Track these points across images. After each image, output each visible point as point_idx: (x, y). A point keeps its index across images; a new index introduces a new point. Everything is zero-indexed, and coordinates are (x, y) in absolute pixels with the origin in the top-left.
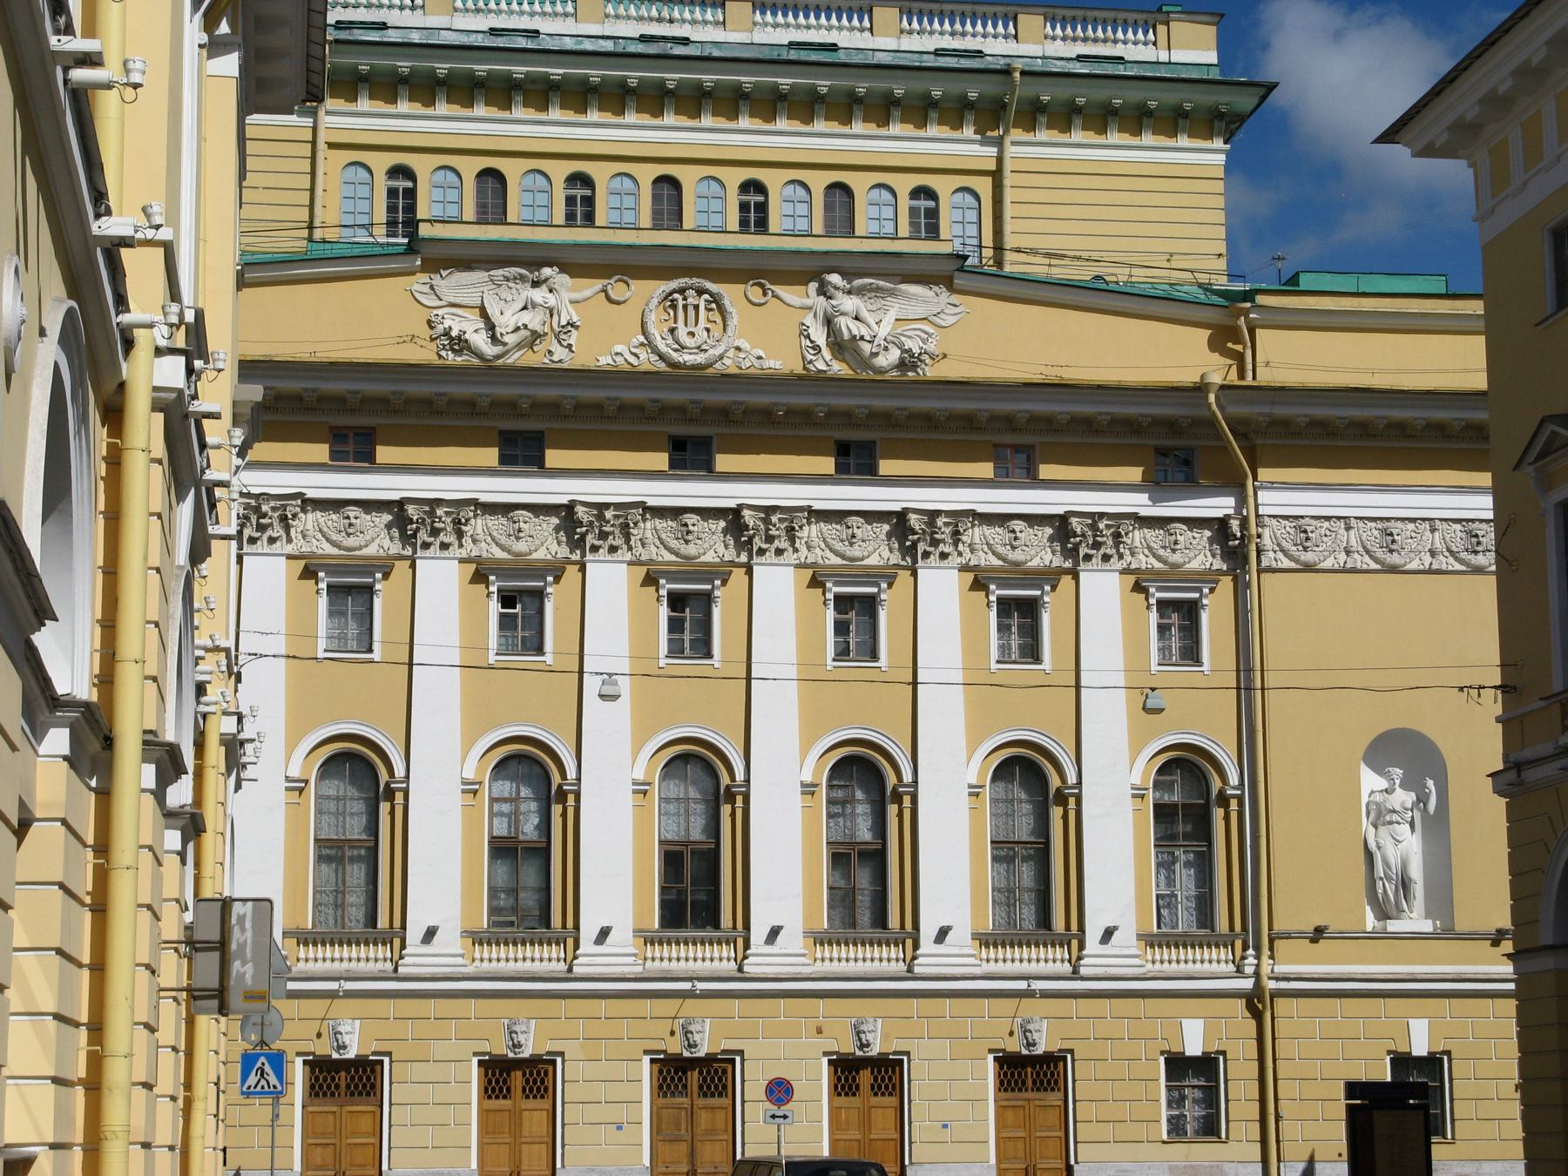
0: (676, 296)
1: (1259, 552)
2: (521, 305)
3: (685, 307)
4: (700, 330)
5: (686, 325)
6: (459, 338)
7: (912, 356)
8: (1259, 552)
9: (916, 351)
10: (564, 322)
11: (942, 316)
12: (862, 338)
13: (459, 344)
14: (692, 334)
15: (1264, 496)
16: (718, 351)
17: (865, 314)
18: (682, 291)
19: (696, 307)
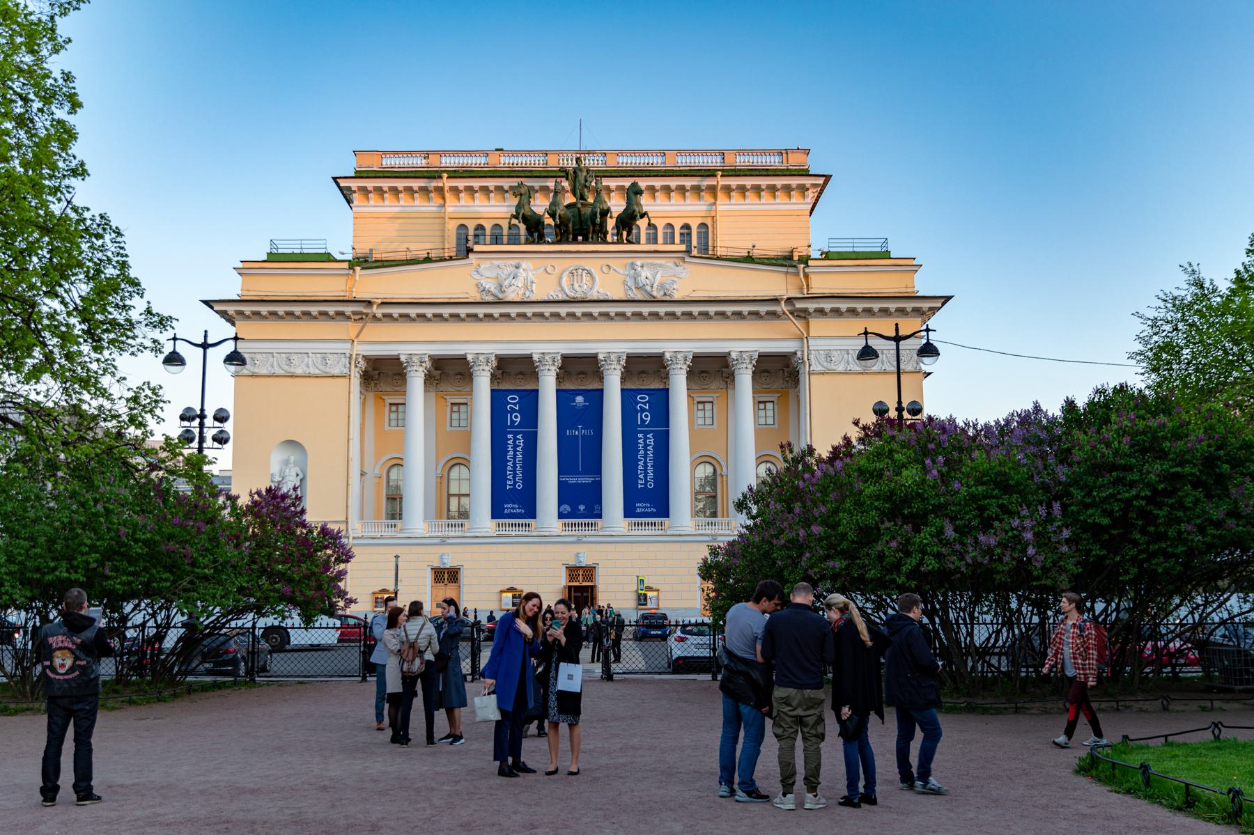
8: (810, 365)
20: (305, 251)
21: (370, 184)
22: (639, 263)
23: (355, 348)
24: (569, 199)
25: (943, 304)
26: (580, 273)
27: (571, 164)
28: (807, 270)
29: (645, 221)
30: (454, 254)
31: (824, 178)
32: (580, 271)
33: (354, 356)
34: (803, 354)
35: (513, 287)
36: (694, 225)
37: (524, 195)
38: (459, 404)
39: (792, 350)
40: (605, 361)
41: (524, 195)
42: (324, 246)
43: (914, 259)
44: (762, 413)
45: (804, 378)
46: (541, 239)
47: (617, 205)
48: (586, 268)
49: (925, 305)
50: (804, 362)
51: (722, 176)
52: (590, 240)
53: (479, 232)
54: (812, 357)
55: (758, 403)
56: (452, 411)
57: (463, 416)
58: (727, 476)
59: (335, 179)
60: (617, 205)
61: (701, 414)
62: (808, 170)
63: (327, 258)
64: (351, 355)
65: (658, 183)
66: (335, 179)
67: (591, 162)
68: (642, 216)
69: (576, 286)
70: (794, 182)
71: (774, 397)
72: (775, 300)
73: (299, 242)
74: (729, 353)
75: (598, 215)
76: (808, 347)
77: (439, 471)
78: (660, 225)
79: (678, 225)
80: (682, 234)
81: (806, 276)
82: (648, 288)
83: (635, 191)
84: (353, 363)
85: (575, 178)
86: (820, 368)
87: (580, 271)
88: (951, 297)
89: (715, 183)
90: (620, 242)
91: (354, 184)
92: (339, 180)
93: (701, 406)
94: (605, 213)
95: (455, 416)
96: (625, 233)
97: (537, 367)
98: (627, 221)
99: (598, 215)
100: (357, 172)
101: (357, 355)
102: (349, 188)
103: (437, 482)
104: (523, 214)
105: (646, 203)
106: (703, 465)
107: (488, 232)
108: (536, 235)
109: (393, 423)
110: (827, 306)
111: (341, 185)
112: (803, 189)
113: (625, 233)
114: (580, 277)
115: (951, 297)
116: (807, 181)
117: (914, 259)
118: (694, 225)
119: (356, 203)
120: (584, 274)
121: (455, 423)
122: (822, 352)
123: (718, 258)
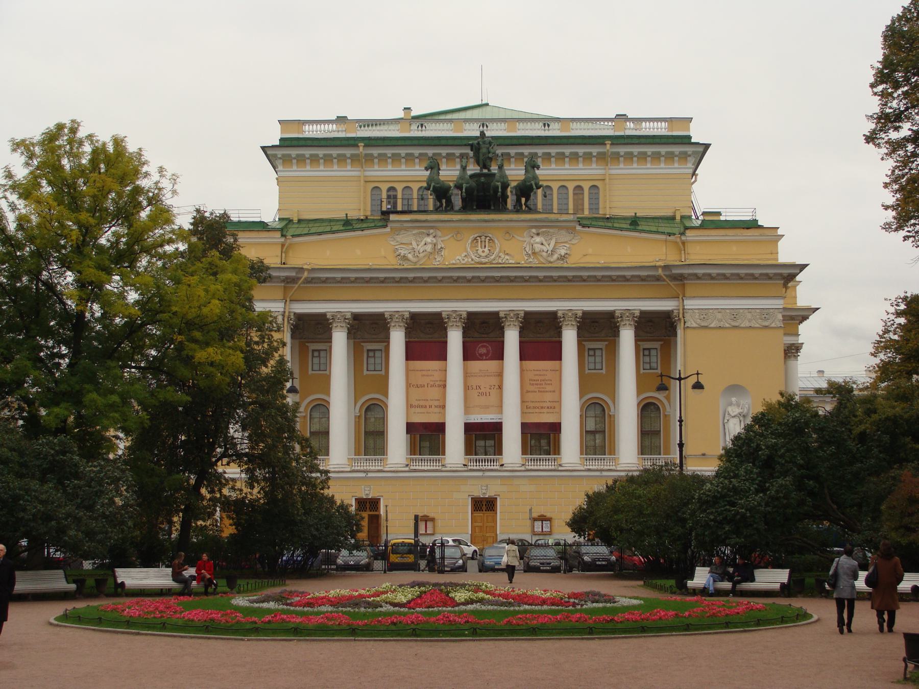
0: (478, 238)
1: (685, 322)
2: (423, 243)
3: (481, 241)
4: (486, 250)
5: (481, 247)
6: (404, 256)
7: (561, 256)
8: (685, 322)
9: (563, 254)
10: (439, 248)
11: (573, 240)
12: (543, 251)
13: (405, 258)
14: (483, 251)
15: (685, 301)
16: (492, 257)
17: (544, 243)
18: (480, 237)
19: (485, 241)
20: (243, 220)
21: (294, 152)
22: (534, 231)
23: (287, 308)
24: (473, 169)
25: (801, 271)
26: (483, 240)
27: (472, 131)
28: (683, 238)
29: (540, 191)
30: (369, 213)
31: (704, 146)
32: (483, 237)
33: (287, 314)
34: (679, 313)
35: (425, 253)
36: (586, 186)
37: (433, 166)
38: (374, 351)
39: (670, 308)
40: (506, 317)
41: (433, 166)
42: (259, 215)
43: (778, 228)
44: (647, 359)
45: (680, 332)
46: (449, 208)
47: (515, 173)
48: (490, 235)
49: (786, 271)
50: (679, 319)
51: (612, 144)
52: (492, 208)
53: (391, 193)
54: (688, 317)
55: (641, 353)
56: (368, 357)
57: (378, 361)
58: (614, 415)
59: (263, 148)
60: (515, 173)
61: (592, 359)
62: (689, 137)
63: (261, 226)
64: (284, 312)
65: (553, 150)
66: (263, 148)
67: (494, 131)
68: (538, 187)
69: (480, 250)
70: (677, 149)
71: (657, 345)
72: (655, 268)
73: (237, 212)
74: (614, 312)
75: (500, 190)
76: (684, 306)
77: (357, 410)
78: (555, 186)
79: (571, 186)
80: (574, 194)
81: (683, 243)
82: (544, 254)
83: (532, 165)
84: (286, 319)
85: (479, 149)
86: (695, 325)
87: (483, 237)
88: (807, 265)
89: (606, 150)
90: (518, 209)
91: (280, 153)
92: (266, 149)
93: (591, 353)
94: (505, 186)
95: (371, 361)
96: (523, 200)
97: (446, 323)
98: (526, 190)
99: (500, 190)
100: (281, 140)
101: (289, 312)
102: (275, 156)
103: (355, 422)
104: (434, 186)
105: (544, 172)
106: (593, 405)
107: (399, 196)
108: (444, 201)
109: (316, 367)
110: (700, 271)
111: (268, 153)
112: (684, 157)
113: (523, 200)
114: (483, 243)
115: (807, 265)
116: (689, 149)
117: (778, 228)
118: (586, 186)
119: (280, 168)
120: (487, 240)
121: (371, 367)
122: (697, 311)
123: (609, 222)
